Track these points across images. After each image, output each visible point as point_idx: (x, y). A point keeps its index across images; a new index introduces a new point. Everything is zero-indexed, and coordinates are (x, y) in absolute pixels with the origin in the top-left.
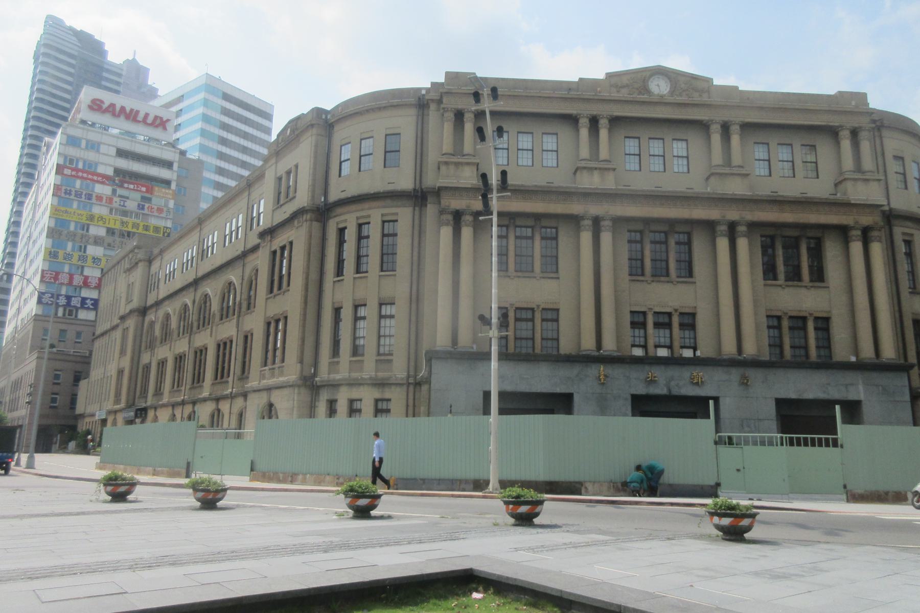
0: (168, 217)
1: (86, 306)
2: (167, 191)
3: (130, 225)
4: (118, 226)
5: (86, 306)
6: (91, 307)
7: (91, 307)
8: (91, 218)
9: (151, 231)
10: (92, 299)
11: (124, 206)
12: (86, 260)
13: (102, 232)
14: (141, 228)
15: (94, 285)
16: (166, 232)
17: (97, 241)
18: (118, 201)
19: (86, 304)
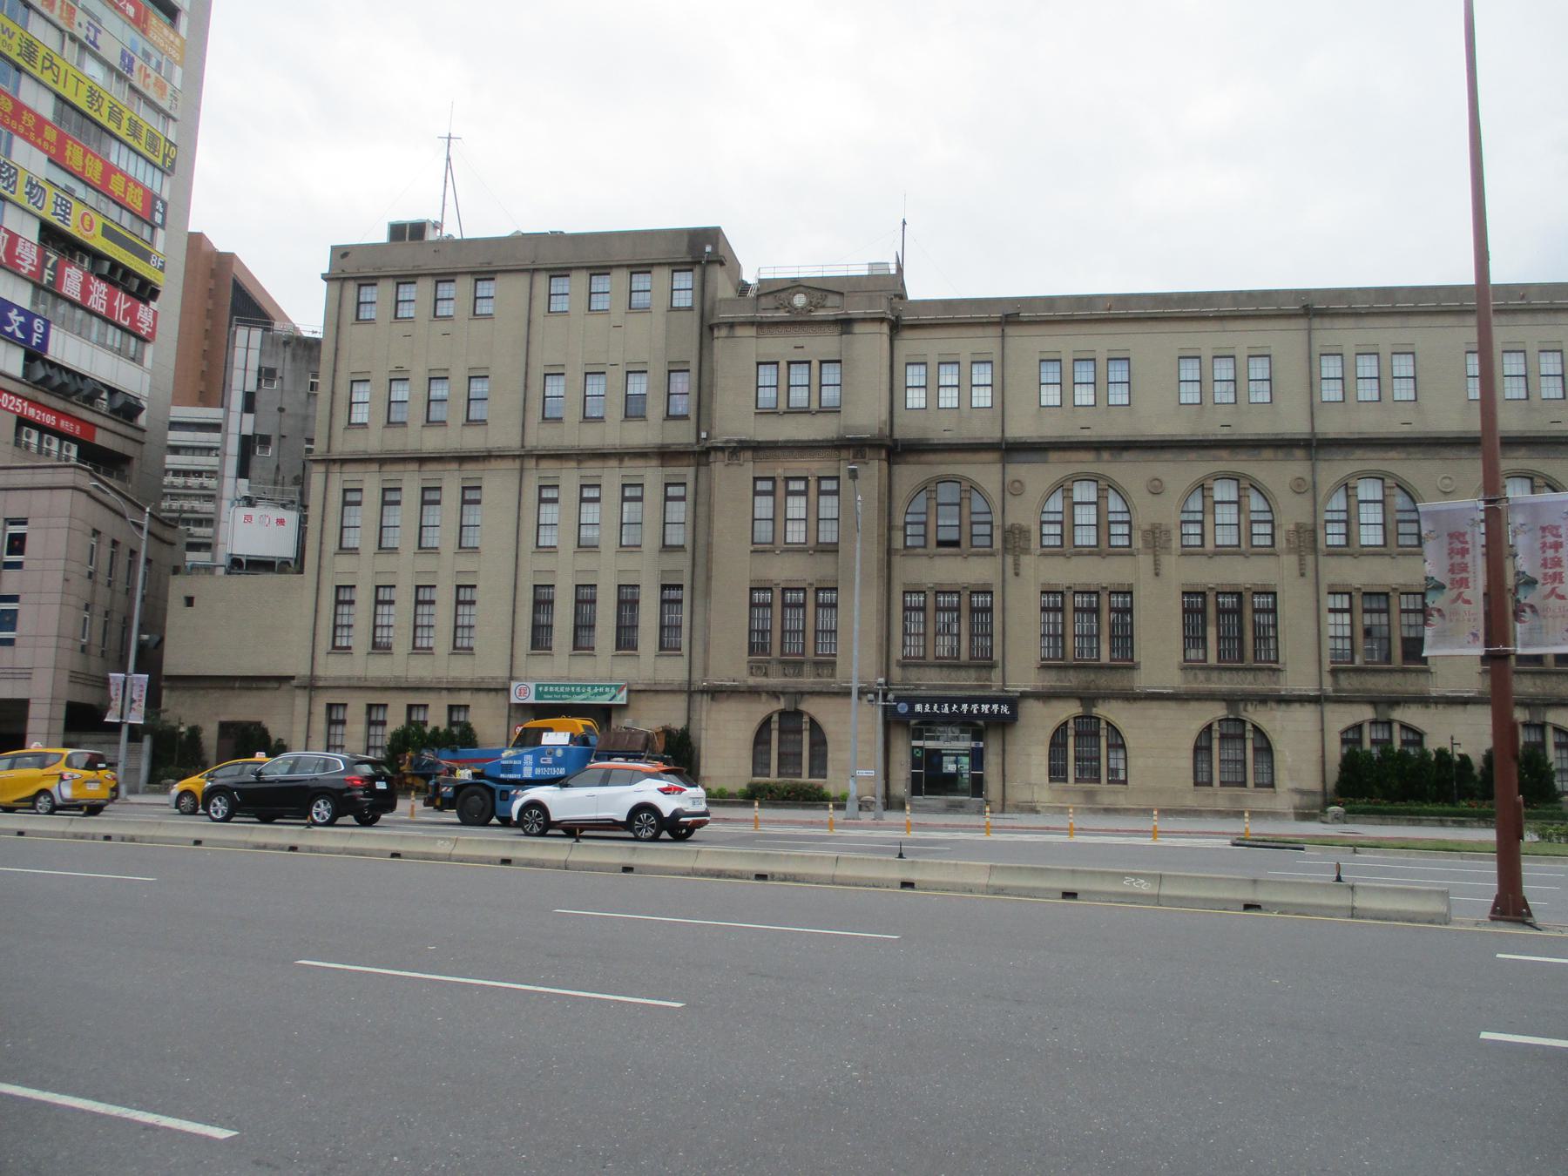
0: (172, 113)
1: (9, 329)
2: (172, 37)
3: (105, 110)
4: (81, 102)
5: (9, 329)
6: (19, 335)
7: (19, 335)
8: (30, 50)
9: (143, 142)
10: (22, 311)
11: (94, 43)
12: (14, 182)
13: (45, 107)
14: (125, 123)
15: (27, 267)
16: (168, 155)
17: (35, 131)
18: (85, 25)
19: (9, 323)
